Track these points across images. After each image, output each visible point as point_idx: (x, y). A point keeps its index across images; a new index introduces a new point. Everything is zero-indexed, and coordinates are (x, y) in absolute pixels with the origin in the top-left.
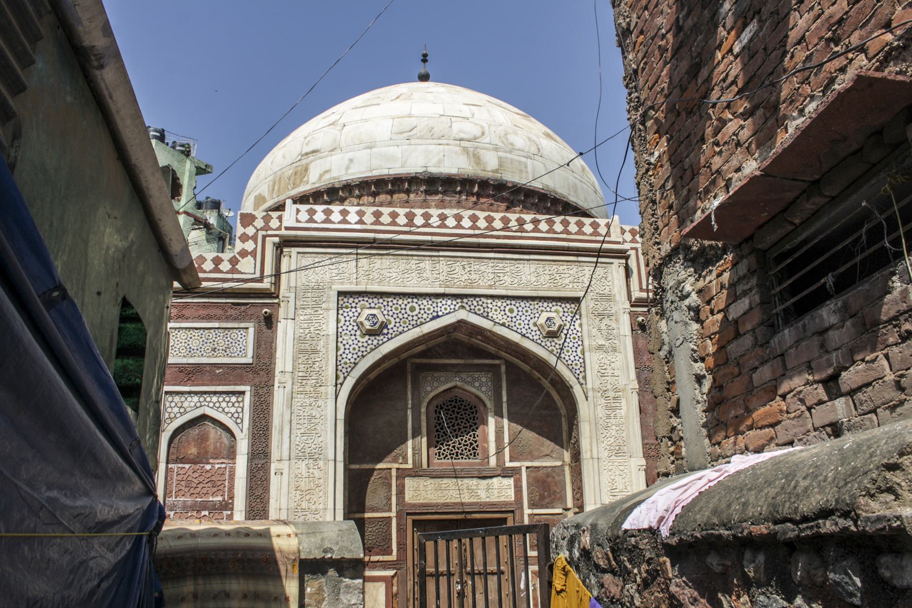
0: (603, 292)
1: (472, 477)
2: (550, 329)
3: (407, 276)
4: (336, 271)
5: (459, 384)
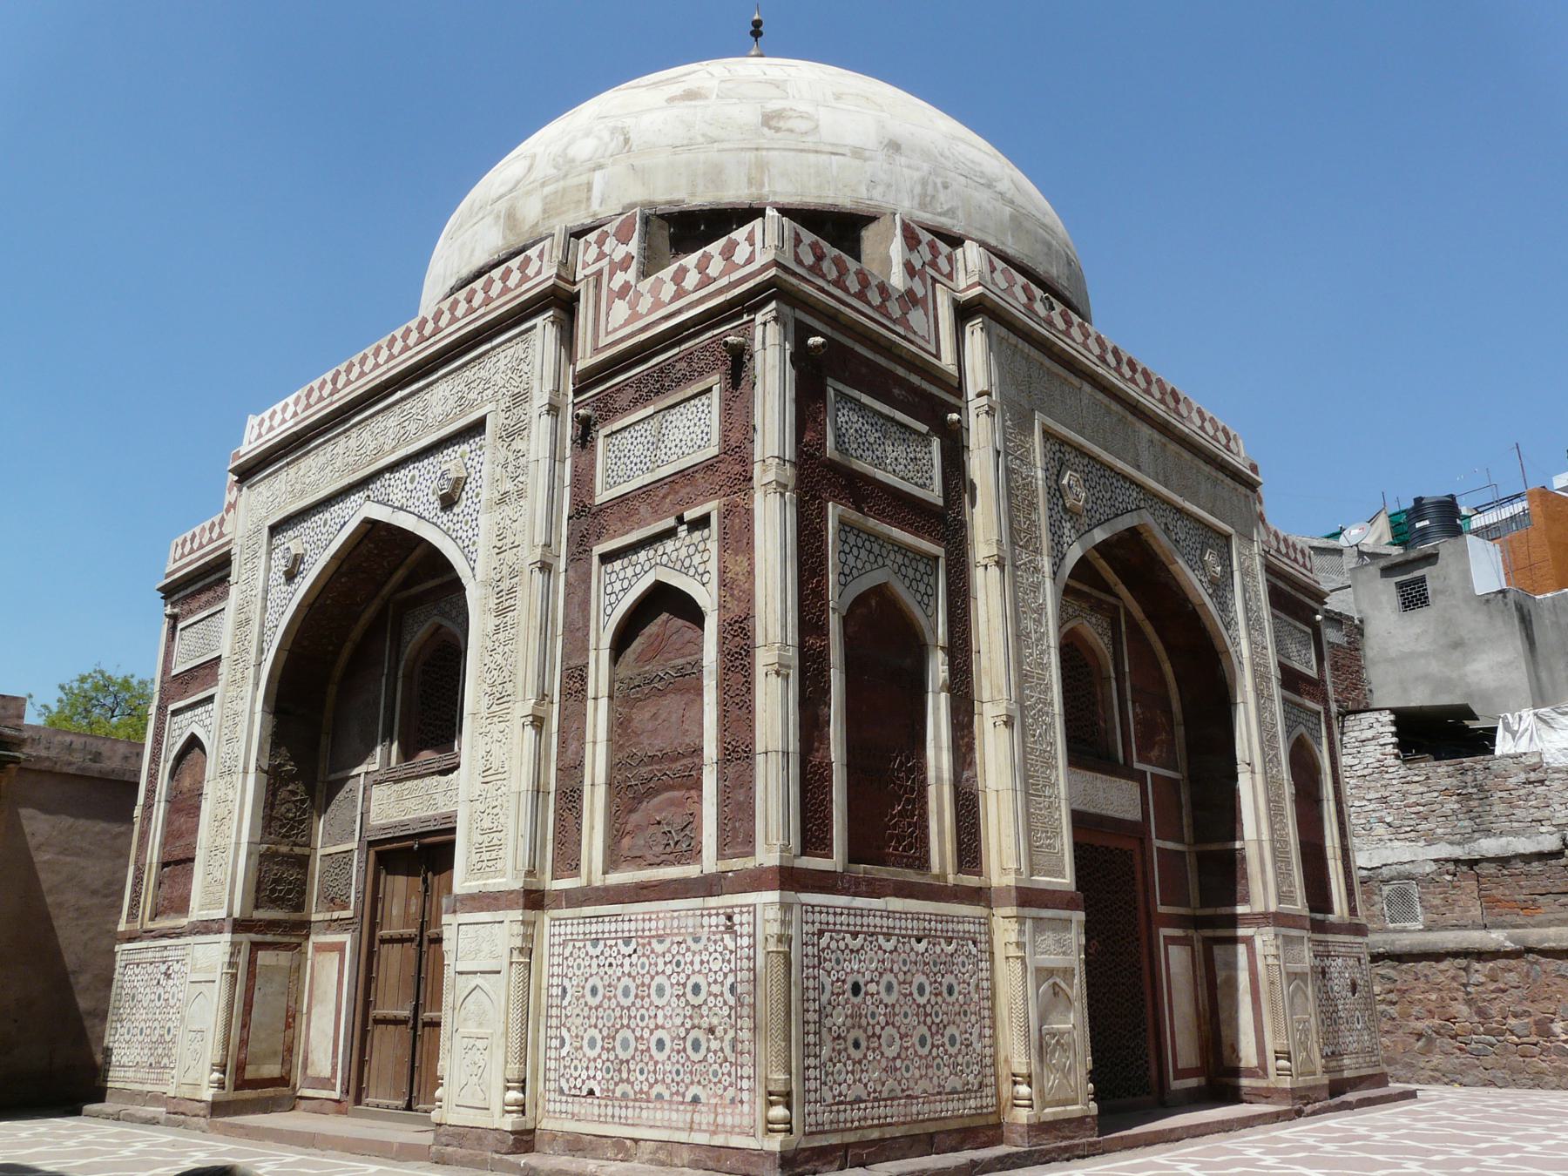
0: (517, 391)
1: (433, 774)
2: (444, 491)
3: (322, 473)
4: (271, 499)
5: (437, 619)
